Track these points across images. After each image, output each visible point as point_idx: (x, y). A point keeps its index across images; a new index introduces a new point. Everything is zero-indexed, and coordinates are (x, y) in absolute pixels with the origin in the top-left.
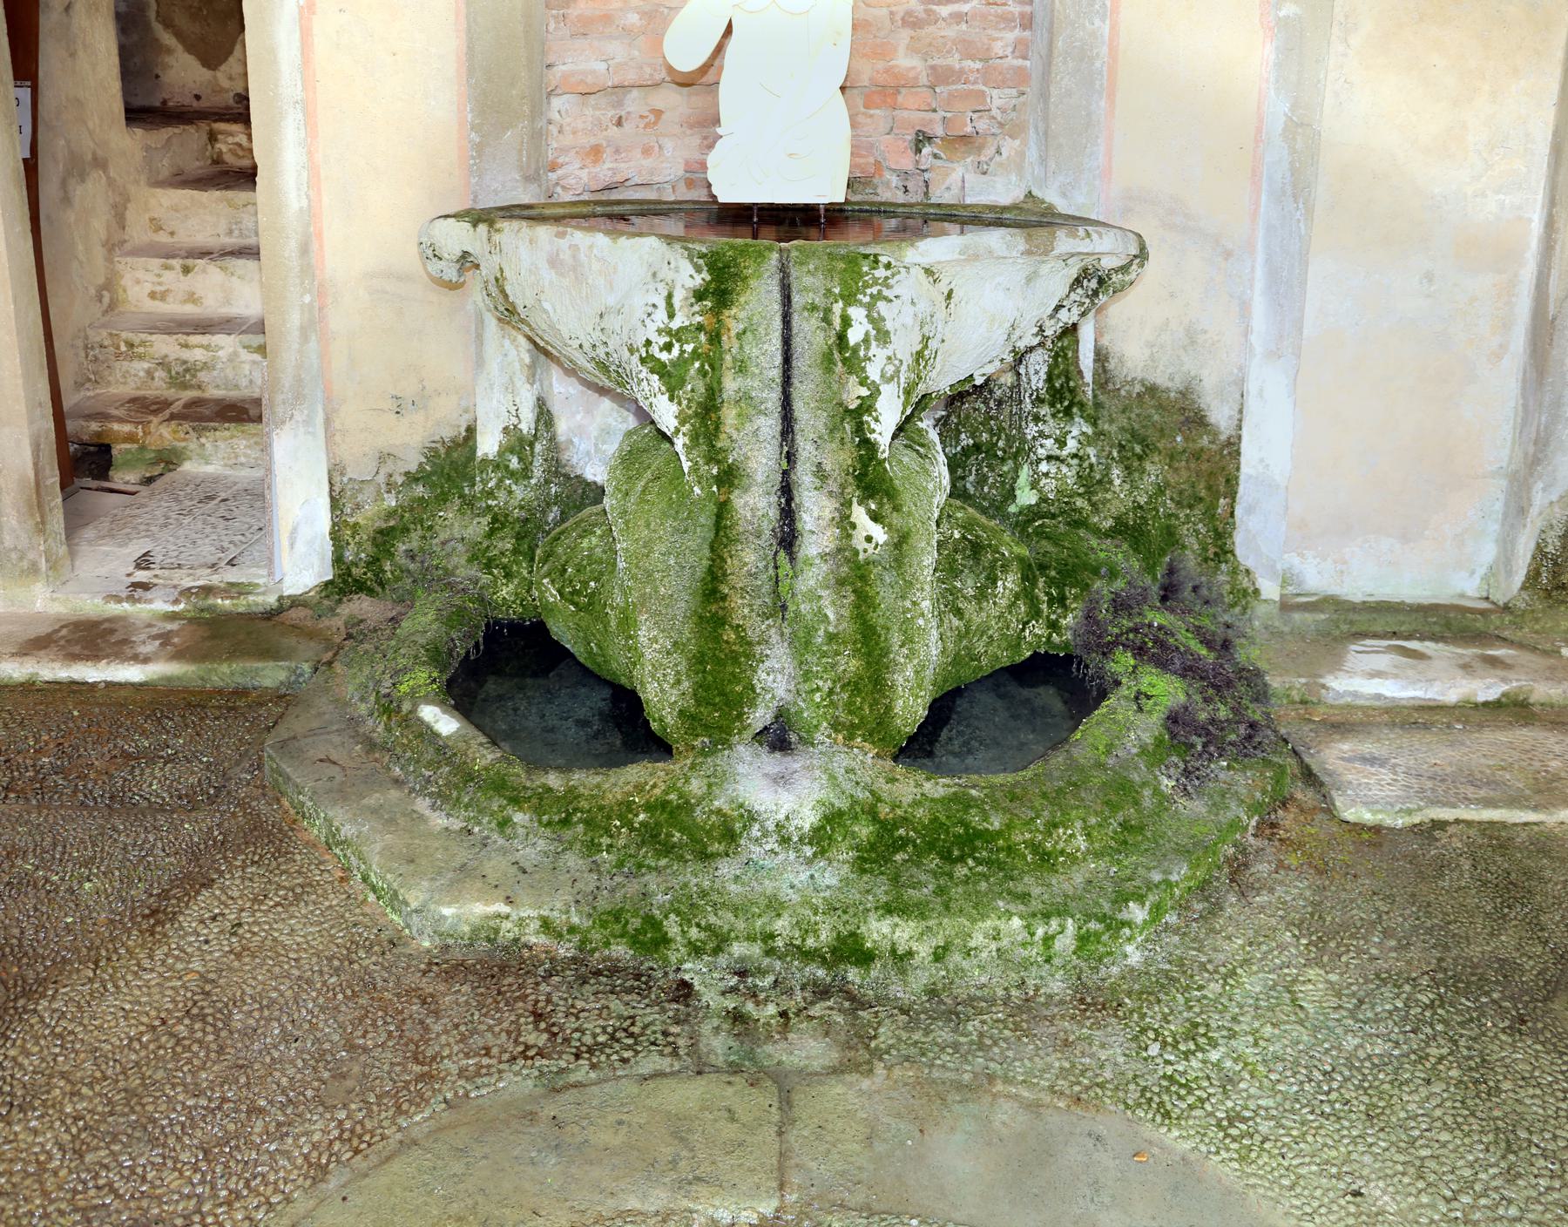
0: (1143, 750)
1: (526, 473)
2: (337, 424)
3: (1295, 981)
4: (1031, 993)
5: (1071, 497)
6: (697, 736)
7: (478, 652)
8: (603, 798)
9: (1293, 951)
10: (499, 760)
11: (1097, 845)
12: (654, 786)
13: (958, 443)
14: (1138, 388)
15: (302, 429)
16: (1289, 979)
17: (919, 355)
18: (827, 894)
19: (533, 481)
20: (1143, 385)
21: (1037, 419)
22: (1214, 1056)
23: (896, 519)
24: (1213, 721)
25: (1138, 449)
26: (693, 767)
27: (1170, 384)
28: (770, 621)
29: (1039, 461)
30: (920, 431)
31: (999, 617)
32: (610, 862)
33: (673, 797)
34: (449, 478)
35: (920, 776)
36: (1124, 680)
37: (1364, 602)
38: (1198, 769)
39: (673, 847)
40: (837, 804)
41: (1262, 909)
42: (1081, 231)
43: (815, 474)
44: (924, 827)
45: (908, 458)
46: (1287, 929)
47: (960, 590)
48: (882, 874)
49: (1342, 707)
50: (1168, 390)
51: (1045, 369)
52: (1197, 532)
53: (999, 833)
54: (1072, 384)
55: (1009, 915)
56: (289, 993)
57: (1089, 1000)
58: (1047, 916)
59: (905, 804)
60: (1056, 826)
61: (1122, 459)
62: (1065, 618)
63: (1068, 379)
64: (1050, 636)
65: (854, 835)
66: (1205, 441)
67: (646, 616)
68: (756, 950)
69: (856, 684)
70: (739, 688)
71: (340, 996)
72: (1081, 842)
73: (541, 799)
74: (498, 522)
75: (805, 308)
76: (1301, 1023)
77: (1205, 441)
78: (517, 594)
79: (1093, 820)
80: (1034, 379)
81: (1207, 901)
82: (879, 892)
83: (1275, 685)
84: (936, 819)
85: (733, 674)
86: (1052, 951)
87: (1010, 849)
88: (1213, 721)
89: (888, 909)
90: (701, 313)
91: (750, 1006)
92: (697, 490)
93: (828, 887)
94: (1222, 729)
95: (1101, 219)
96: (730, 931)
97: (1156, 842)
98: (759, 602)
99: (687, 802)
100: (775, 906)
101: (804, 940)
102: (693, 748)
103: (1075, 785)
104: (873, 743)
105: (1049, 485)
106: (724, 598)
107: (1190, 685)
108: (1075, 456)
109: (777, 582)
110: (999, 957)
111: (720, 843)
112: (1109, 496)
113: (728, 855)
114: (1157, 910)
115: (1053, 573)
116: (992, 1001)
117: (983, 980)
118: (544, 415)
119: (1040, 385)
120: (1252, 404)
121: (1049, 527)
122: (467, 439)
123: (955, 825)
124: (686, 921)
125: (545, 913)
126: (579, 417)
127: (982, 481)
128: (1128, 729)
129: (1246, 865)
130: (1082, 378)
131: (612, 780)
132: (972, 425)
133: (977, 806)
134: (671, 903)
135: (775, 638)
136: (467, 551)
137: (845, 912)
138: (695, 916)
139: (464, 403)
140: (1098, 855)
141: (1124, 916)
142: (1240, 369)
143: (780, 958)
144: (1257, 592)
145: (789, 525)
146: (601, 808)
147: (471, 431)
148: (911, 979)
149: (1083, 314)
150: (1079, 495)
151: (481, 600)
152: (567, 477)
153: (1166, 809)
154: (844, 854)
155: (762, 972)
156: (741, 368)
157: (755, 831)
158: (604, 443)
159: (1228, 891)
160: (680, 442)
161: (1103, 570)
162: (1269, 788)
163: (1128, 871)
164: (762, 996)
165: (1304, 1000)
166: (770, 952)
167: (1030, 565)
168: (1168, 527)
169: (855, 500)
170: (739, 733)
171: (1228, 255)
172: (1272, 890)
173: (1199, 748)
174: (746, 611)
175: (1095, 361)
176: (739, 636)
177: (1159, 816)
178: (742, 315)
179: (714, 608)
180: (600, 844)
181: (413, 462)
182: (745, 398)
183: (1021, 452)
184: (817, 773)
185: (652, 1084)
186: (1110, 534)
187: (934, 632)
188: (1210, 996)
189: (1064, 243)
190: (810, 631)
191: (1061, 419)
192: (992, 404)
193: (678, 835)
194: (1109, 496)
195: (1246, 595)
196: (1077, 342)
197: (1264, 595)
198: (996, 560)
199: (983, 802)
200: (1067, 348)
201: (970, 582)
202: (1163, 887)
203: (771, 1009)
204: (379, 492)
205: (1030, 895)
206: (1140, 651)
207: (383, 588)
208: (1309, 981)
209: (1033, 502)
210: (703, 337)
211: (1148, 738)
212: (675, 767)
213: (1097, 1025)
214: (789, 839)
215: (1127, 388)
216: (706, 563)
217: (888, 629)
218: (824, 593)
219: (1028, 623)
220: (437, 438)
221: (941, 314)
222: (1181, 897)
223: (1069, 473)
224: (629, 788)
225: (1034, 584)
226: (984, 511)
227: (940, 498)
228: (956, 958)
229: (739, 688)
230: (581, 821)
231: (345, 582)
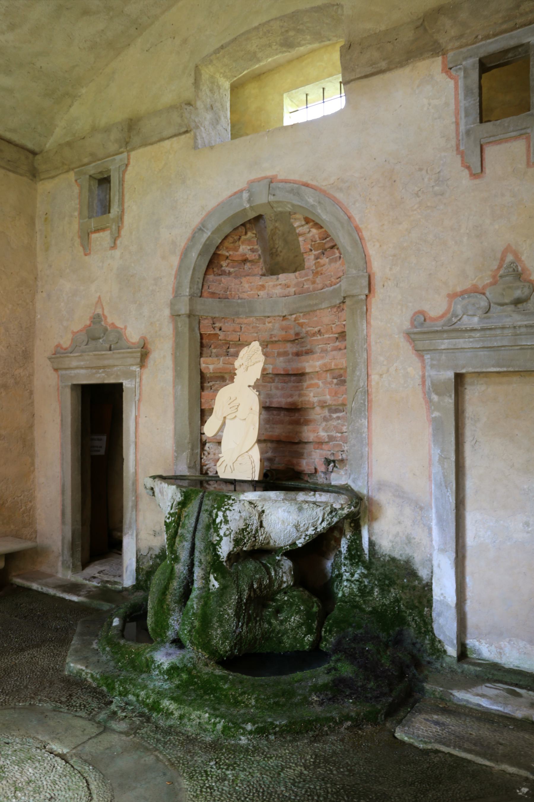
20: (390, 557)
27: (401, 558)
40: (178, 665)
50: (400, 560)
54: (359, 553)
55: (206, 712)
58: (217, 717)
63: (357, 551)
65: (181, 677)
75: (204, 510)
77: (416, 582)
120: (435, 569)
125: (92, 672)
130: (364, 551)
143: (139, 703)
148: (168, 721)
223: (355, 587)
228: (186, 720)
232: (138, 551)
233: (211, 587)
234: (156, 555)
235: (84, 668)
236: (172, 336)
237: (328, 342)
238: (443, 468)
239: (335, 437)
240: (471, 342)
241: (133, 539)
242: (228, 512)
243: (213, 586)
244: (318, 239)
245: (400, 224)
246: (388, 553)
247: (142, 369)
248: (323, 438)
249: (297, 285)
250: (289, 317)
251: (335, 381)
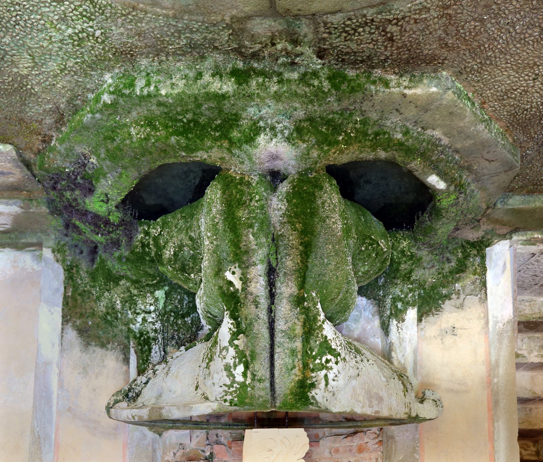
0: (105, 176)
1: (395, 300)
3: (33, 68)
4: (156, 58)
5: (140, 295)
6: (314, 178)
7: (418, 215)
8: (359, 146)
9: (34, 82)
10: (408, 163)
11: (126, 130)
12: (334, 153)
13: (192, 318)
14: (109, 346)
15: (499, 319)
16: (36, 69)
17: (211, 360)
18: (252, 103)
19: (391, 296)
20: (107, 348)
21: (156, 331)
22: (70, 31)
23: (221, 282)
24: (73, 190)
25: (109, 318)
26: (316, 163)
27: (95, 348)
28: (280, 233)
29: (154, 311)
30: (210, 324)
31: (172, 237)
32: (356, 116)
33: (326, 148)
34: (430, 297)
35: (209, 161)
36: (114, 208)
37: (4, 248)
38: (79, 167)
39: (325, 124)
41: (48, 102)
42: (137, 419)
43: (259, 303)
44: (207, 137)
45: (215, 311)
46: (37, 92)
47: (190, 249)
48: (227, 114)
49: (13, 198)
50: (96, 346)
51: (152, 354)
52: (81, 279)
53: (172, 134)
55: (167, 96)
56: (511, 46)
57: (129, 56)
58: (149, 95)
59: (216, 147)
60: (145, 139)
61: (116, 313)
62: (142, 237)
63: (141, 350)
64: (148, 229)
65: (240, 132)
66: (78, 322)
67: (338, 234)
68: (286, 75)
69: (239, 204)
70: (294, 201)
71: (486, 46)
72: (133, 131)
73: (388, 145)
74: (407, 277)
76: (30, 48)
77: (78, 322)
78: (399, 243)
79: (128, 142)
80: (157, 349)
81: (74, 105)
82: (228, 105)
83: (44, 208)
84: (201, 141)
85: (297, 208)
86: (146, 79)
87: (166, 127)
88: (73, 190)
89: (224, 97)
90: (312, 377)
91: (289, 48)
92: (314, 294)
93: (252, 107)
94: (68, 186)
95: (127, 425)
96: (299, 84)
97: (98, 132)
98: (285, 242)
99: (319, 146)
100: (277, 97)
101: (264, 81)
102: (316, 172)
103: (136, 159)
104: (231, 176)
105: (150, 300)
106: (301, 244)
107: (83, 207)
108: (138, 314)
109: (276, 252)
110: (171, 75)
111: (304, 126)
112: (122, 295)
113: (300, 121)
114: (97, 100)
115: (147, 258)
116: (174, 54)
117: (178, 64)
118: (385, 328)
119: (154, 347)
120: (57, 341)
121: (150, 280)
122: (422, 316)
123: (192, 138)
124: (320, 89)
126: (369, 327)
127: (181, 301)
128: (112, 185)
129: (56, 122)
130: (135, 351)
131: (354, 155)
132: (186, 327)
133: (182, 147)
134: (327, 97)
135: (277, 225)
136: (422, 263)
137: (244, 95)
138: (315, 91)
139: (423, 333)
140: (125, 125)
141: (113, 97)
142: (63, 357)
143: (275, 71)
144: (53, 252)
145: (271, 279)
146: (360, 142)
147: (420, 320)
148: (213, 64)
149: (135, 380)
150: (136, 296)
151: (416, 240)
152: (375, 299)
153: (94, 148)
154: (245, 123)
155: (284, 64)
156: (293, 352)
157: (287, 132)
159: (65, 109)
160: (322, 317)
161: (124, 260)
162: (46, 159)
163: (111, 118)
164: (283, 53)
165: (29, 59)
166: (280, 74)
167: (158, 262)
168: (94, 281)
169: (240, 291)
170: (294, 180)
171: (69, 410)
172: (44, 111)
173: (79, 177)
174: (291, 238)
175: (129, 358)
176: (295, 226)
177: (97, 145)
178: (293, 377)
179: (306, 239)
180: (360, 124)
181: (447, 305)
182: (292, 338)
183: (163, 315)
184: (257, 161)
185: (337, 8)
186: (121, 278)
187: (203, 229)
188: (72, 60)
189: (144, 413)
190: (261, 229)
191: (145, 331)
192: (176, 337)
193: (324, 130)
194: (122, 295)
195: (58, 250)
196: (138, 367)
197: (50, 250)
198: (174, 264)
199: (179, 149)
200: (142, 364)
201: (186, 253)
202: (95, 111)
203: (279, 47)
204: (463, 290)
205: (157, 105)
206: (107, 222)
207: (462, 244)
208: (26, 68)
209: (157, 292)
210: (311, 366)
211: (103, 181)
212: (325, 162)
213: (125, 44)
214: (271, 129)
215: (114, 346)
216: (310, 260)
217: (224, 231)
218: (254, 247)
219: (159, 235)
220: (436, 316)
221: (201, 379)
222: (86, 106)
224: (346, 152)
225: (156, 254)
226: (180, 287)
227: (200, 293)
228: (191, 74)
229: (294, 201)
230: (370, 135)
231: (480, 247)
235: (406, 91)
241: (494, 317)
246: (109, 353)
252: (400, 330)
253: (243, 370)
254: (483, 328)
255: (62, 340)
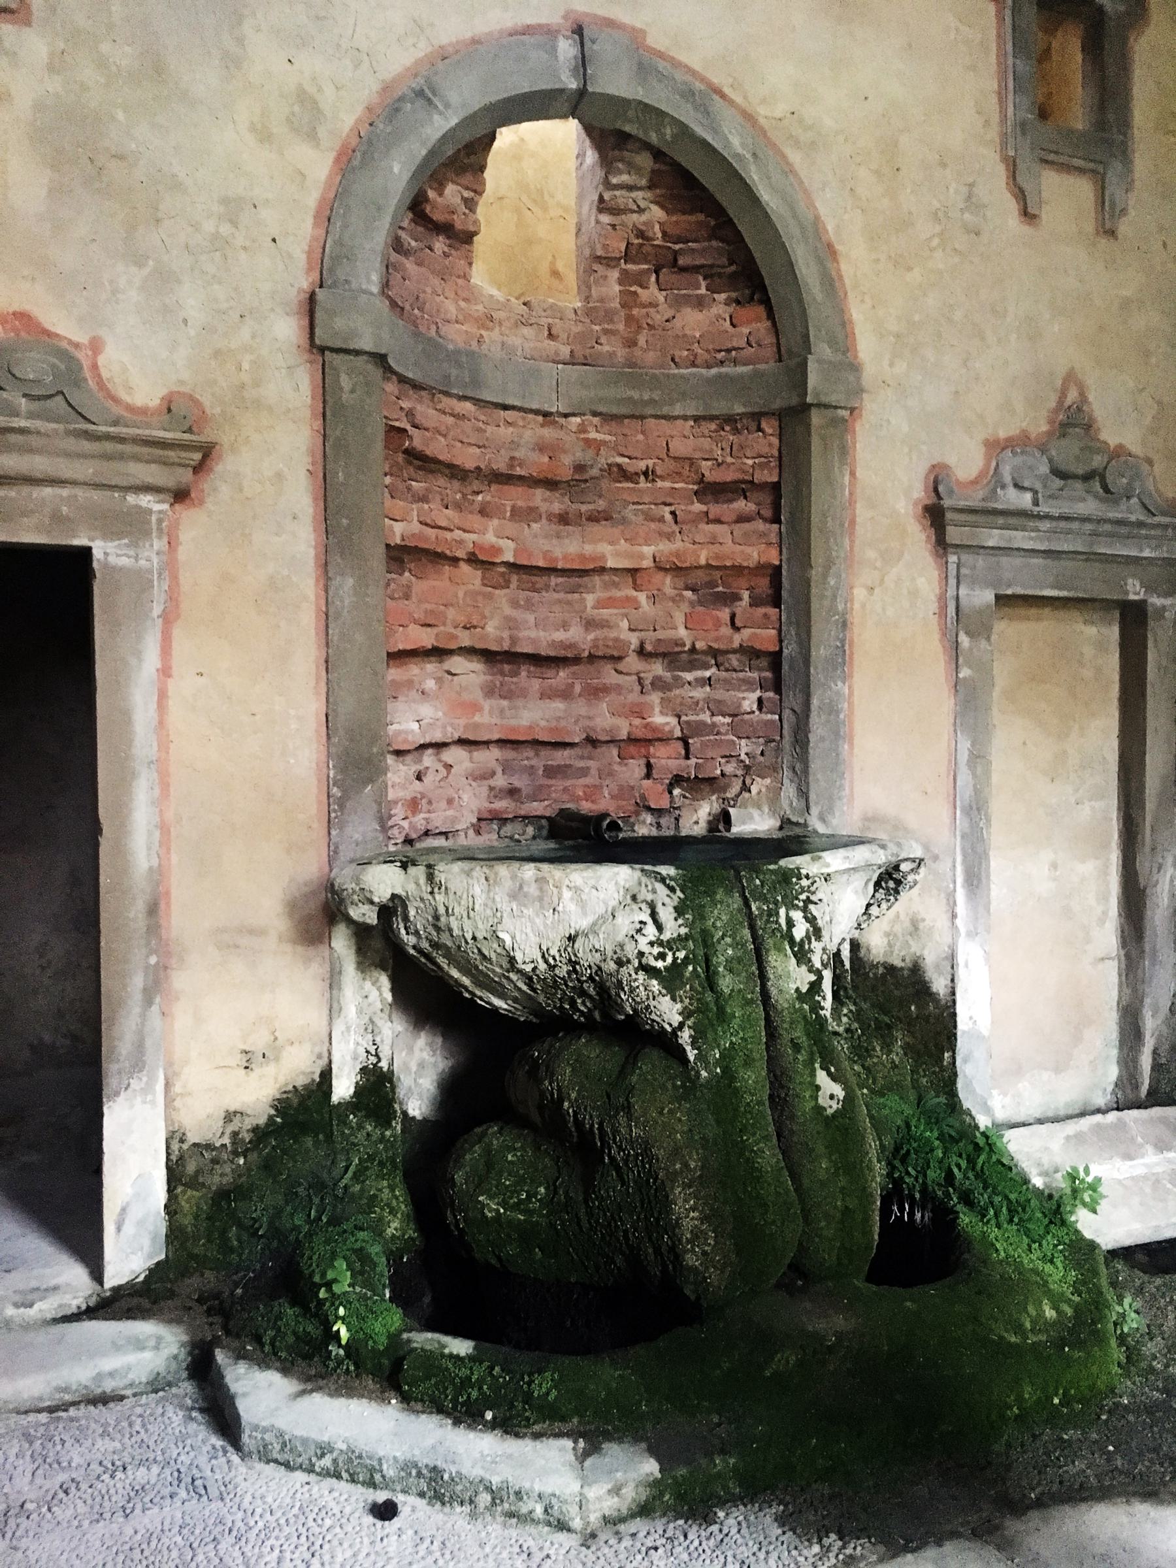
2: (177, 1088)
14: (881, 970)
122: (320, 1084)
139: (317, 1050)
147: (326, 1075)
158: (420, 1077)
175: (851, 951)
220: (290, 1088)
232: (174, 1137)
233: (823, 1101)
234: (255, 1130)
236: (307, 413)
237: (671, 501)
238: (974, 775)
239: (714, 725)
240: (1031, 539)
242: (811, 907)
243: (832, 1097)
244: (659, 235)
245: (910, 269)
247: (177, 506)
248: (667, 728)
249: (581, 337)
250: (562, 420)
251: (689, 594)
252: (372, 1050)
253: (794, 930)
254: (175, 1074)
255: (953, 975)
